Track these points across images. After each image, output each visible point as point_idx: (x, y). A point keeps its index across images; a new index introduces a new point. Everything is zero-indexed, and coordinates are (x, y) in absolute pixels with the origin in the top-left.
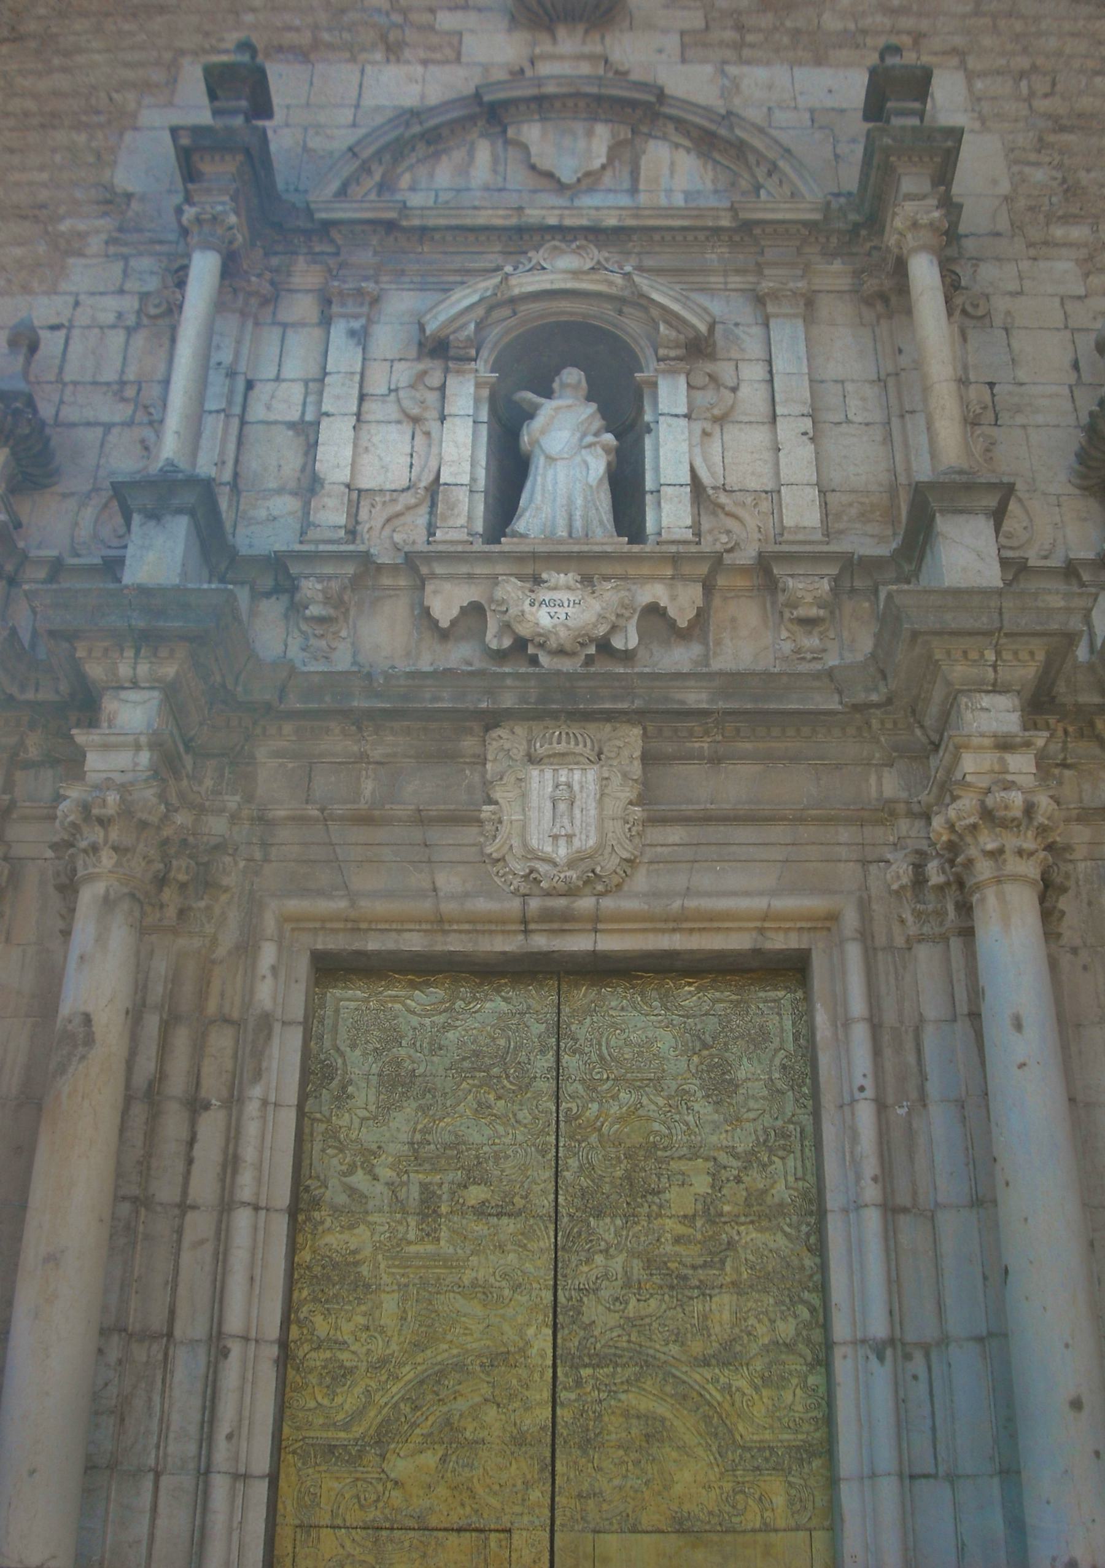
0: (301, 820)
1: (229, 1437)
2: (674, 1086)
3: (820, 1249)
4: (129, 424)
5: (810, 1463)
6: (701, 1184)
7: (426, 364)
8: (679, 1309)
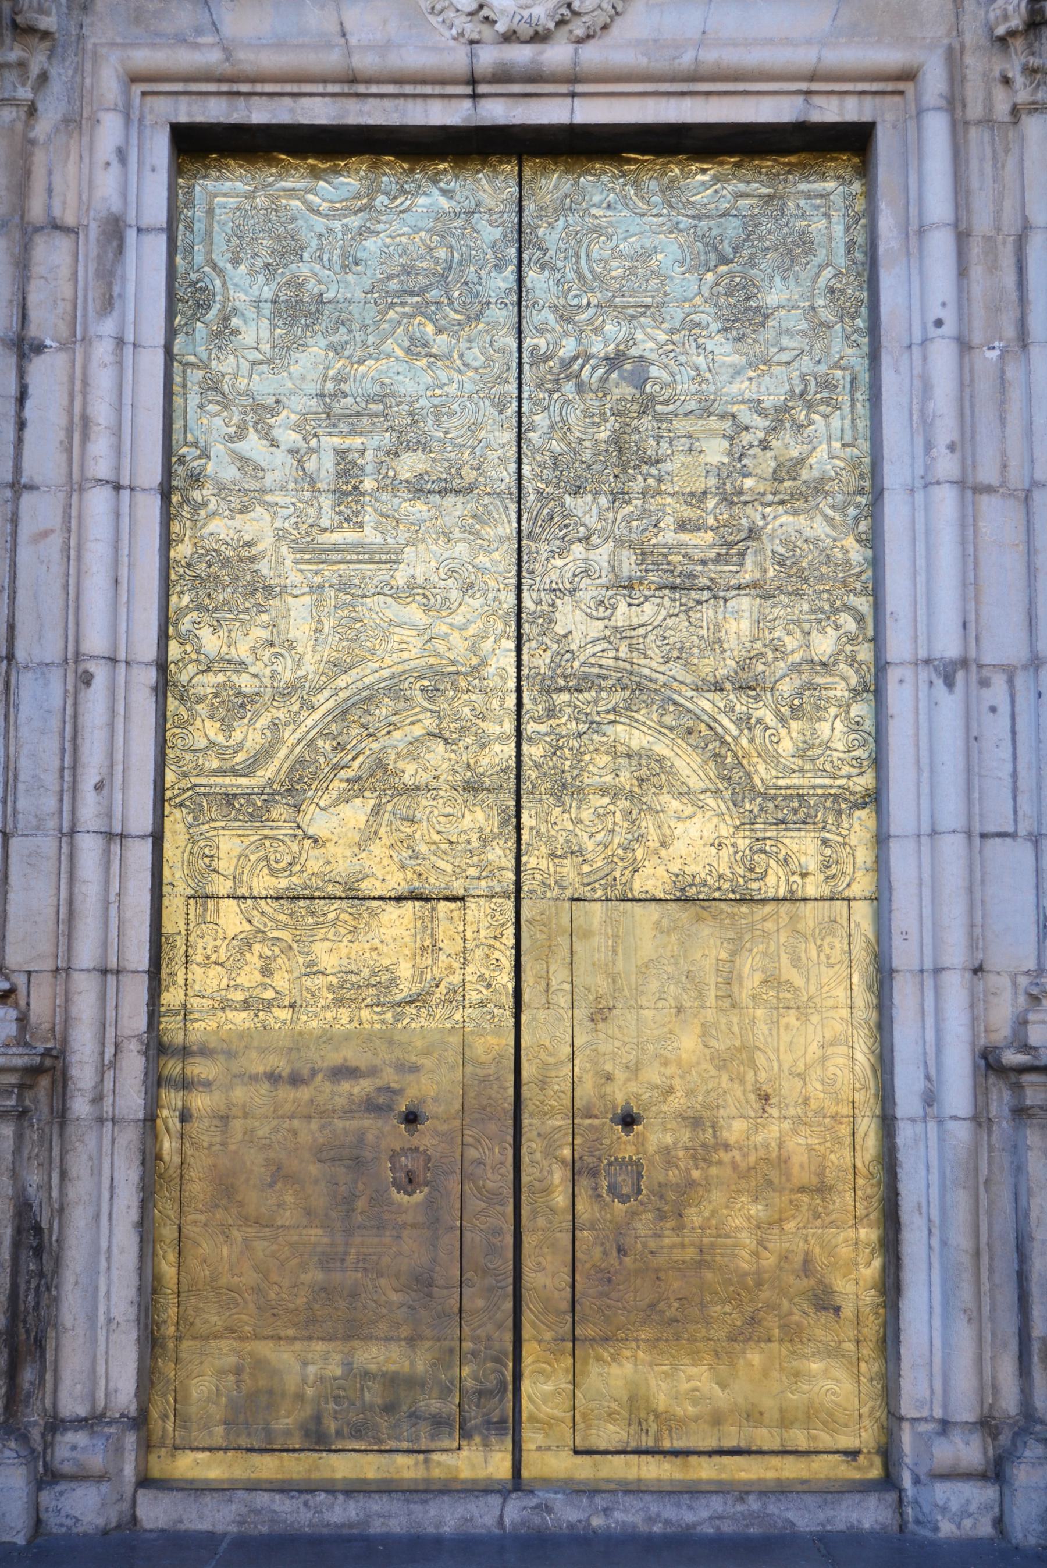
1: (99, 787)
2: (679, 315)
3: (874, 541)
5: (850, 815)
6: (715, 452)
8: (682, 616)
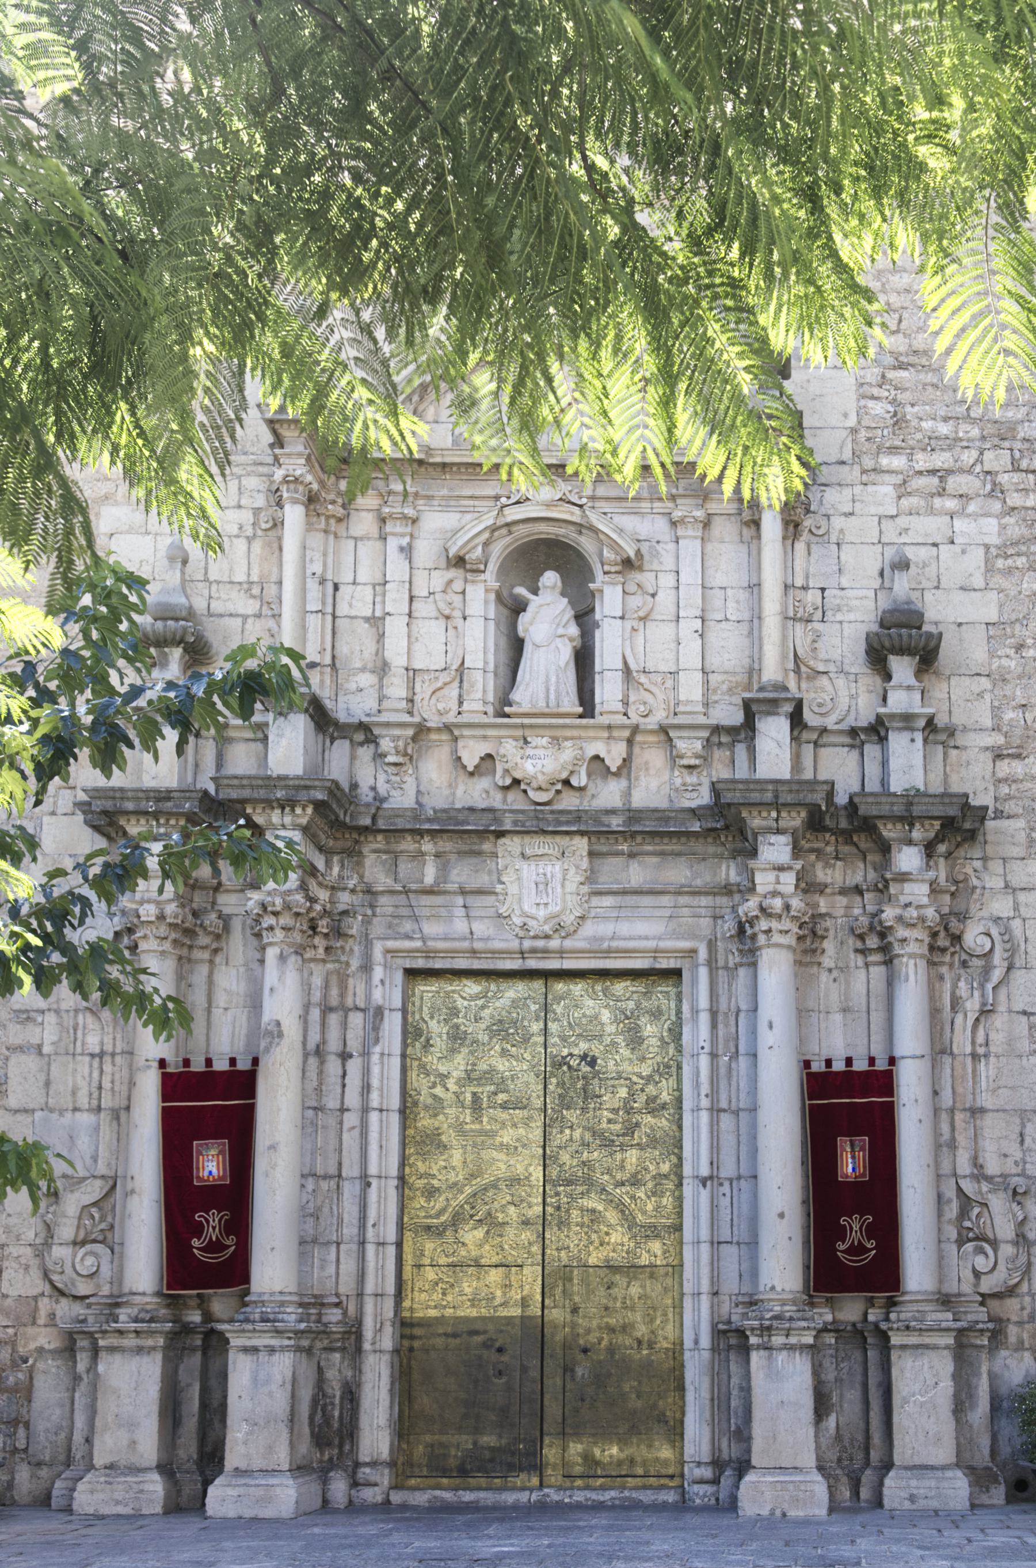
0: (392, 892)
4: (258, 616)
7: (453, 573)
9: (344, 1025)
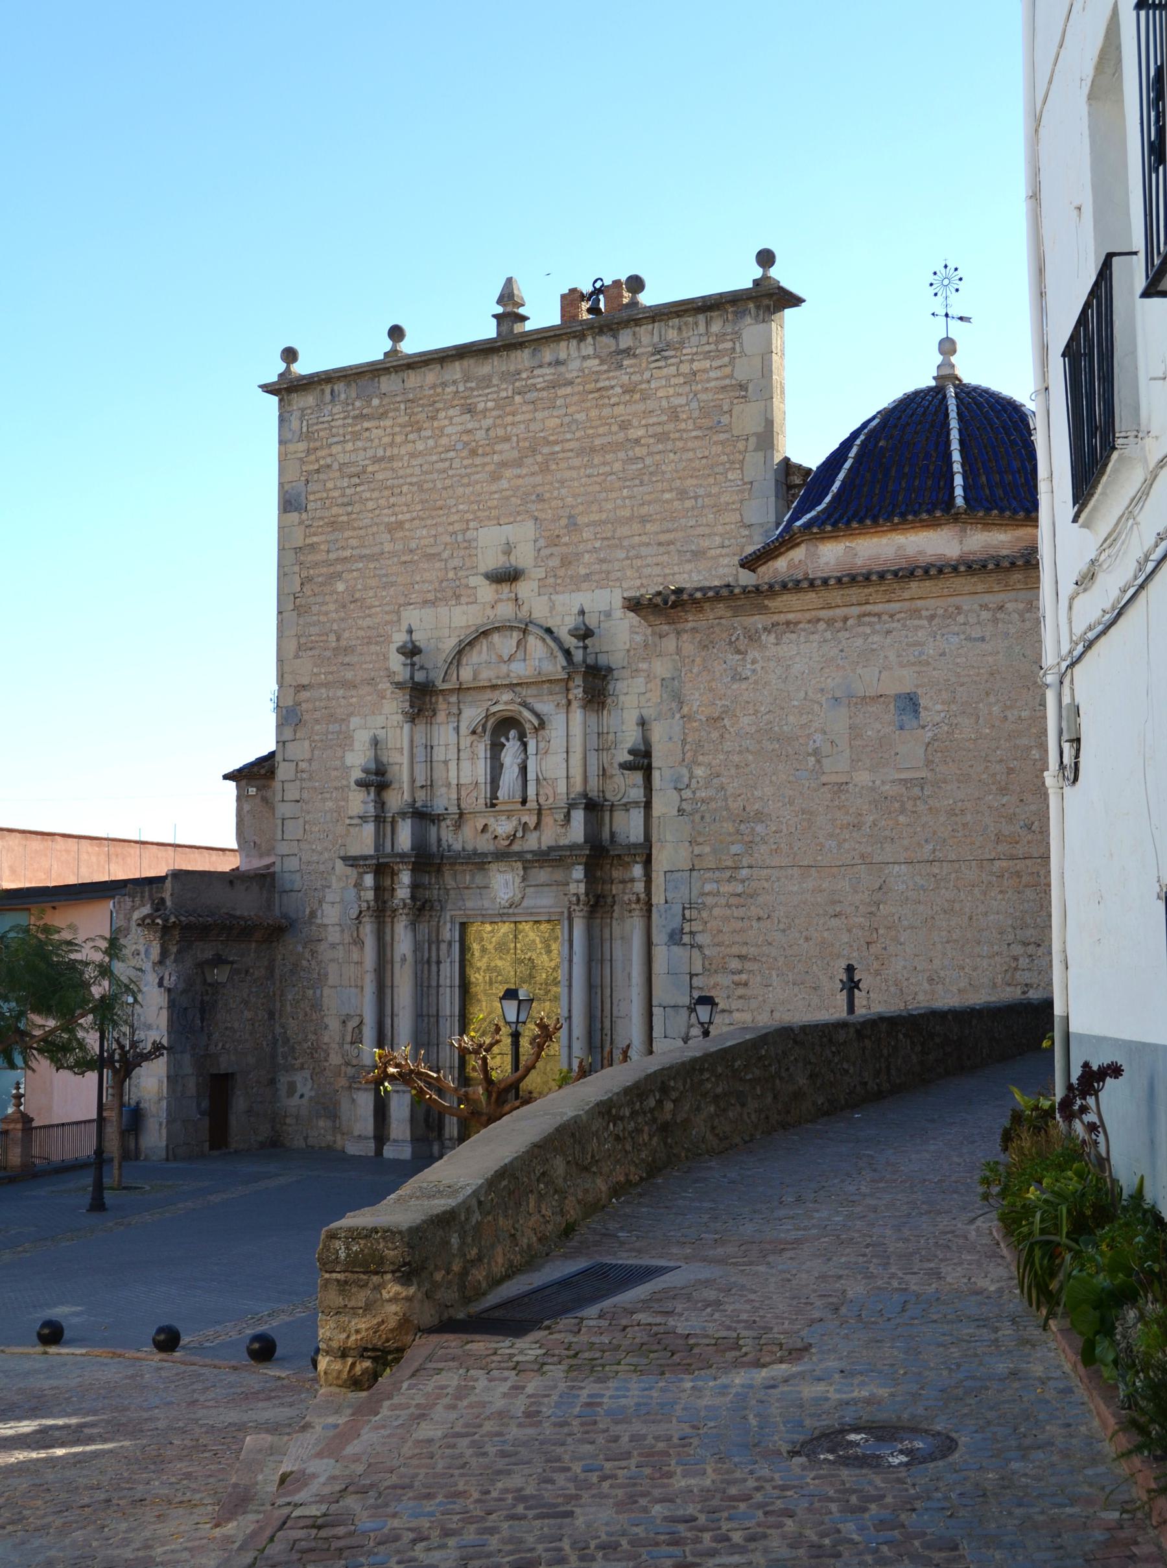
9: (438, 949)
